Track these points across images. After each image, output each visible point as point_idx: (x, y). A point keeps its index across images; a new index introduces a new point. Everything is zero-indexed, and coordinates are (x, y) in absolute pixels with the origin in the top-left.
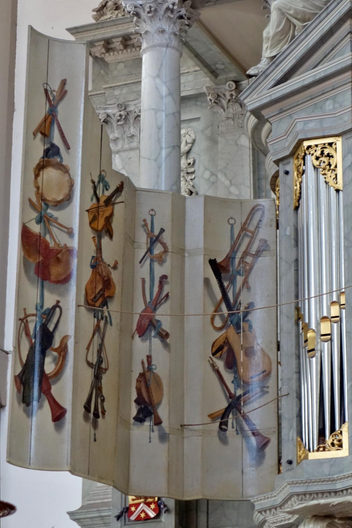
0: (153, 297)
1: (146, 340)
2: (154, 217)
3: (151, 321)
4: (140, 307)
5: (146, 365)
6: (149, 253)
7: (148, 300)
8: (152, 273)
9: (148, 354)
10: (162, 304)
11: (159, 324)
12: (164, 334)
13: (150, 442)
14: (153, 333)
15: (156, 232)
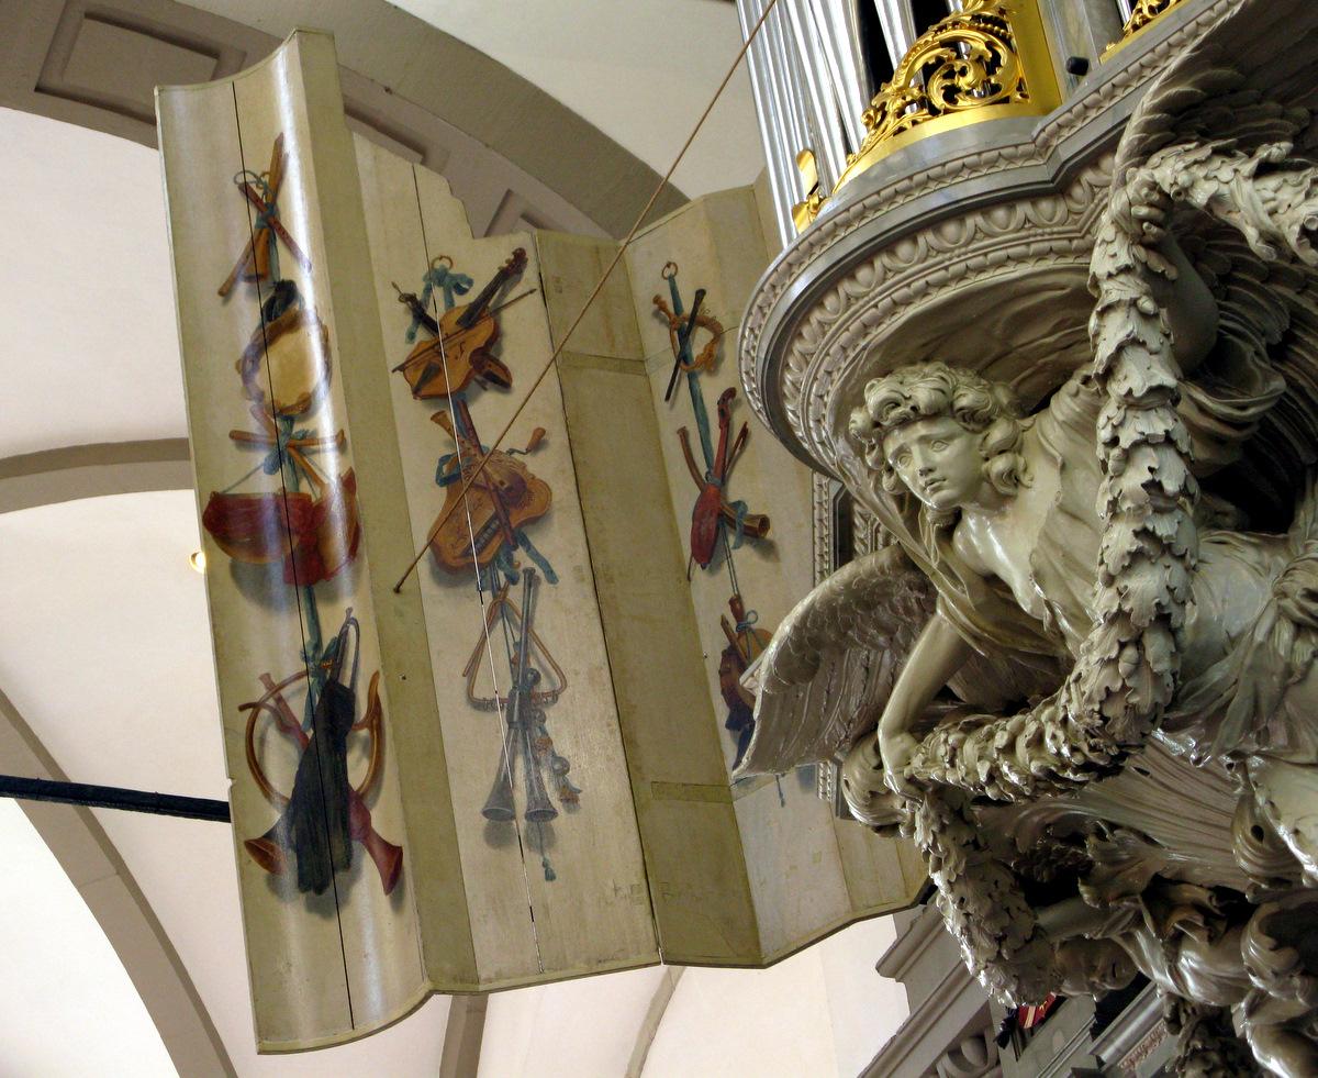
0: (712, 455)
1: (719, 565)
2: (676, 278)
3: (721, 515)
4: (686, 496)
5: (733, 624)
6: (682, 364)
7: (703, 468)
8: (699, 401)
9: (731, 595)
10: (735, 463)
11: (741, 509)
12: (756, 525)
13: (783, 803)
14: (732, 539)
15: (688, 308)
